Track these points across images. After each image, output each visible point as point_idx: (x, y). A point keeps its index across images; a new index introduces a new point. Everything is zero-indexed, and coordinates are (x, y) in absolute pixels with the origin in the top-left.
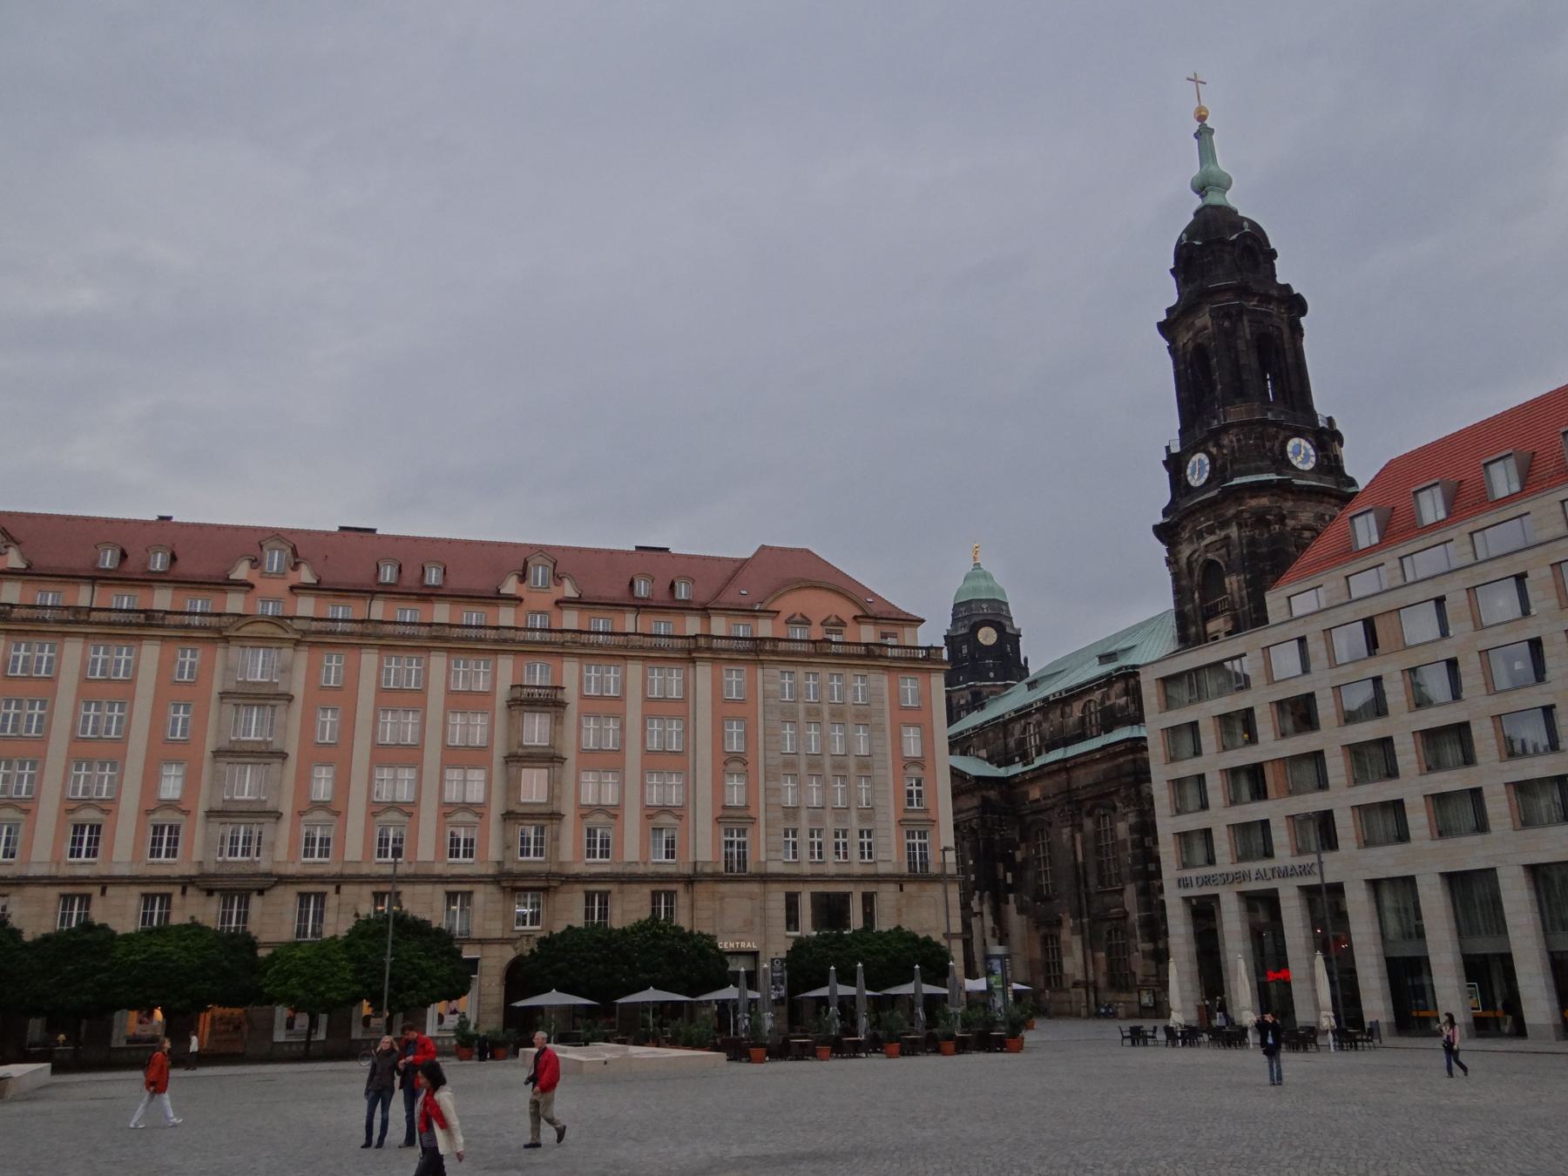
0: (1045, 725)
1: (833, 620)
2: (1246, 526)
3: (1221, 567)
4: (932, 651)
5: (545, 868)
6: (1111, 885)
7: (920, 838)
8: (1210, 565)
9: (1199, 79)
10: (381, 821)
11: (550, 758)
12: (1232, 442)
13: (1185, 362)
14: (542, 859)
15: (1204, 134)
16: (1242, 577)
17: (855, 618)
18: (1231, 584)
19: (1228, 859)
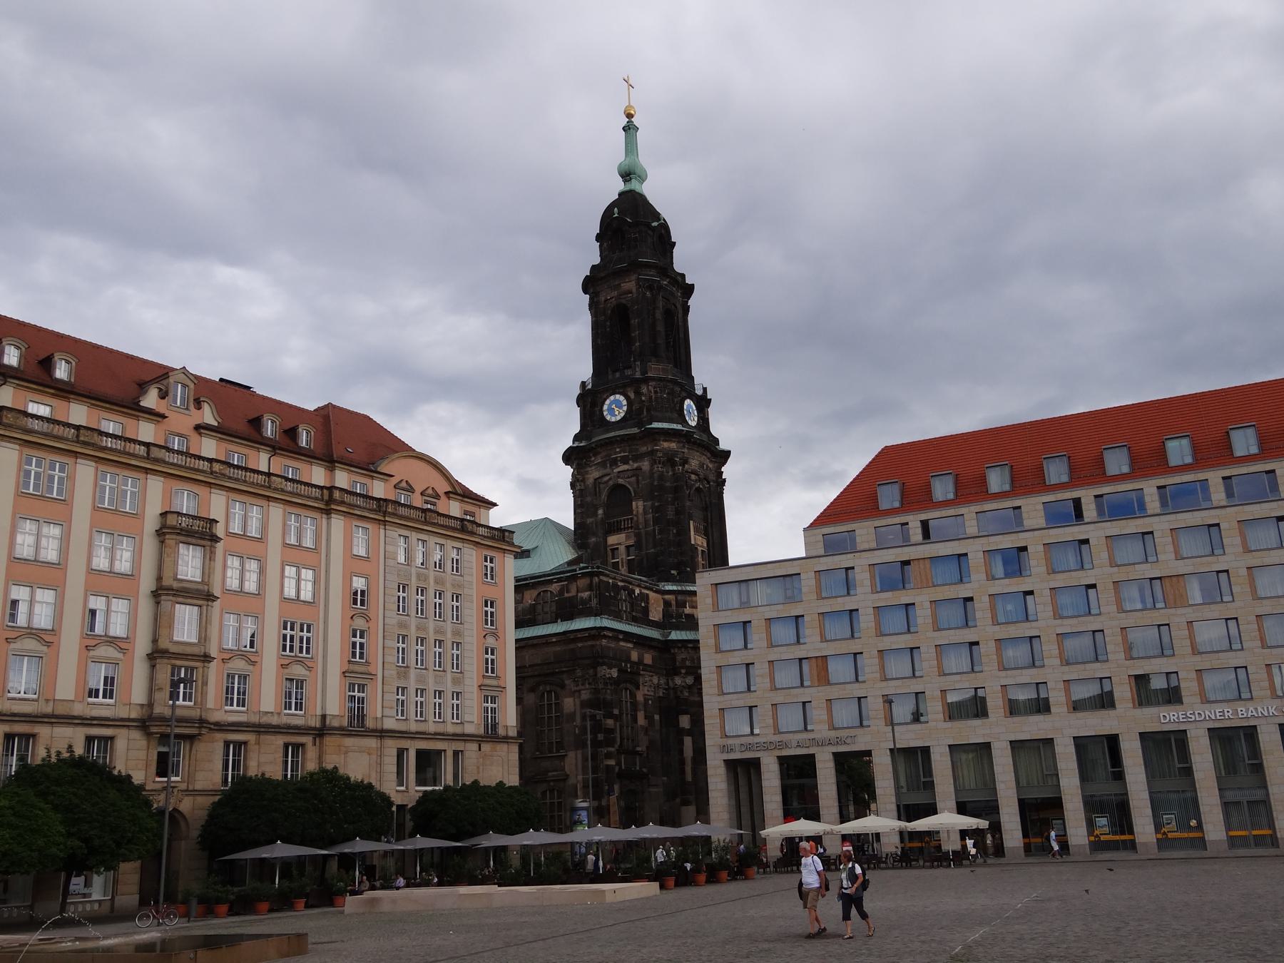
1: (430, 491)
3: (630, 492)
4: (507, 534)
5: (195, 714)
6: (551, 752)
7: (491, 703)
8: (618, 490)
9: (630, 82)
10: (14, 650)
11: (202, 595)
14: (191, 704)
15: (630, 129)
17: (446, 493)
18: (637, 507)
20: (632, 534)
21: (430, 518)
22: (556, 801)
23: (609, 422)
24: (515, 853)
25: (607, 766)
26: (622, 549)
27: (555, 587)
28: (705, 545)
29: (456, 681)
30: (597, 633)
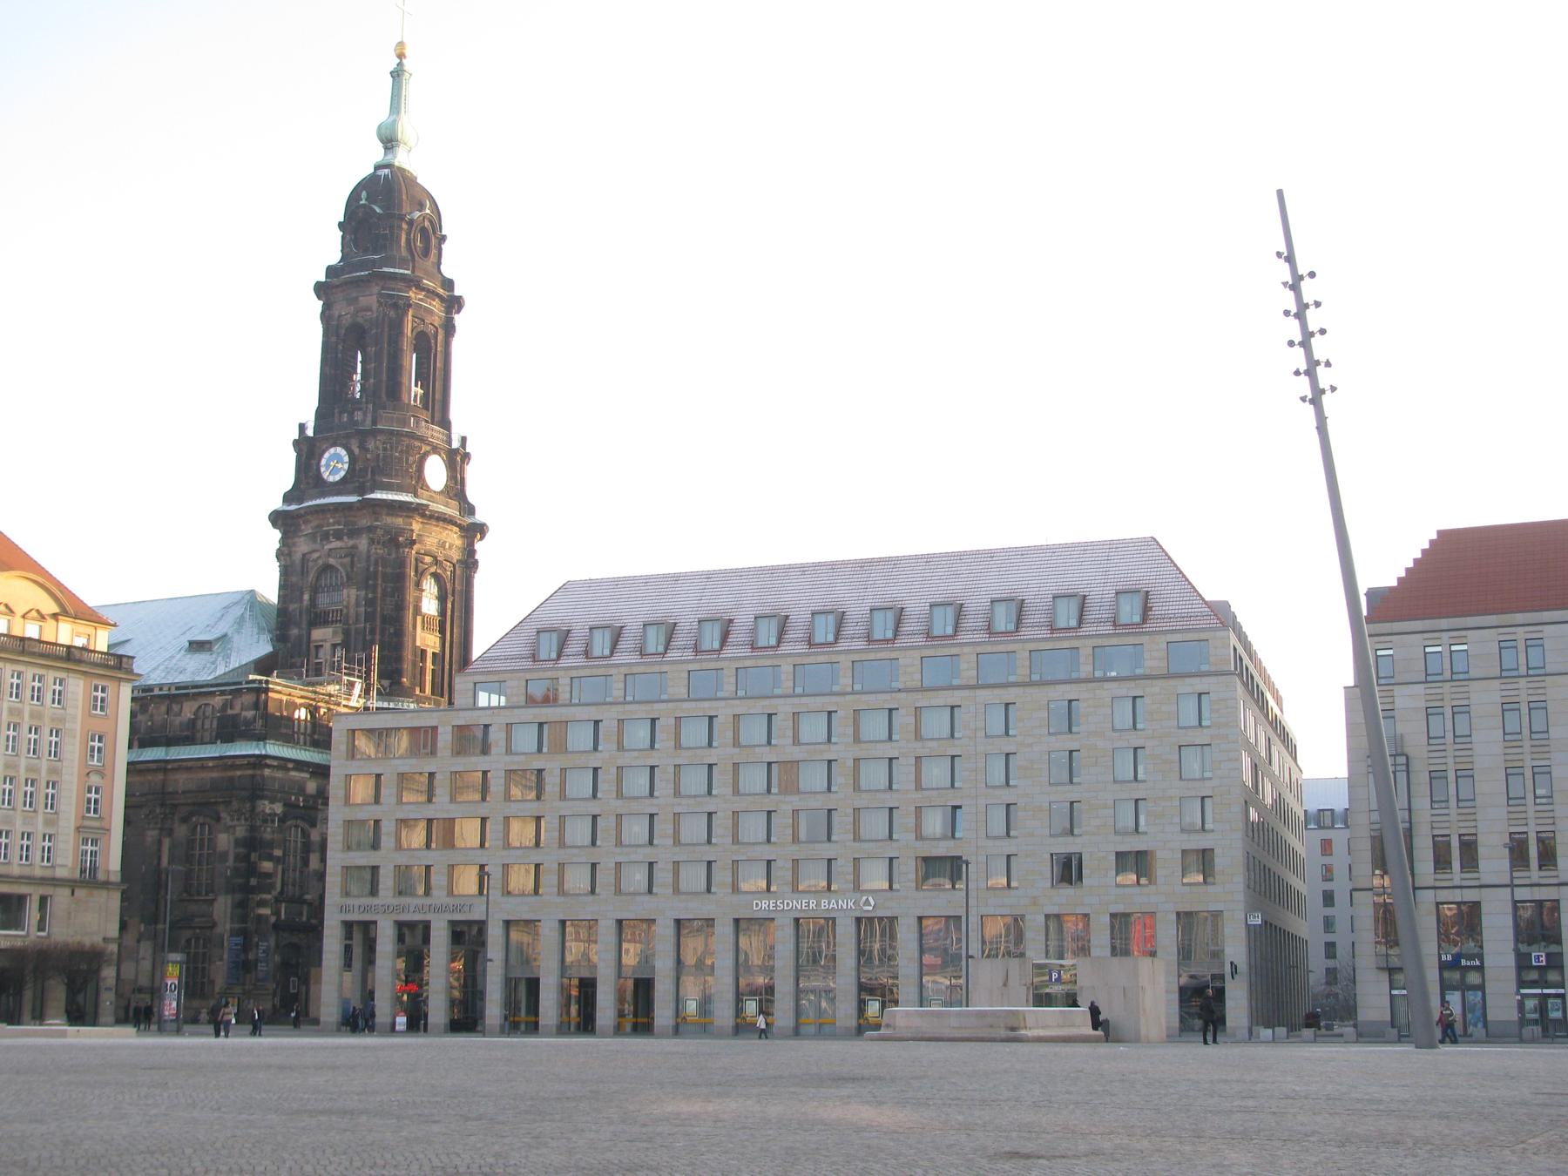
0: (140, 717)
2: (378, 543)
4: (124, 660)
7: (92, 845)
12: (377, 448)
13: (338, 336)
15: (397, 74)
16: (363, 593)
17: (55, 616)
18: (349, 597)
19: (391, 893)
20: (340, 631)
21: (29, 646)
22: (201, 951)
23: (324, 482)
24: (108, 1003)
25: (260, 916)
26: (328, 646)
27: (218, 701)
28: (438, 645)
29: (48, 823)
30: (259, 761)
